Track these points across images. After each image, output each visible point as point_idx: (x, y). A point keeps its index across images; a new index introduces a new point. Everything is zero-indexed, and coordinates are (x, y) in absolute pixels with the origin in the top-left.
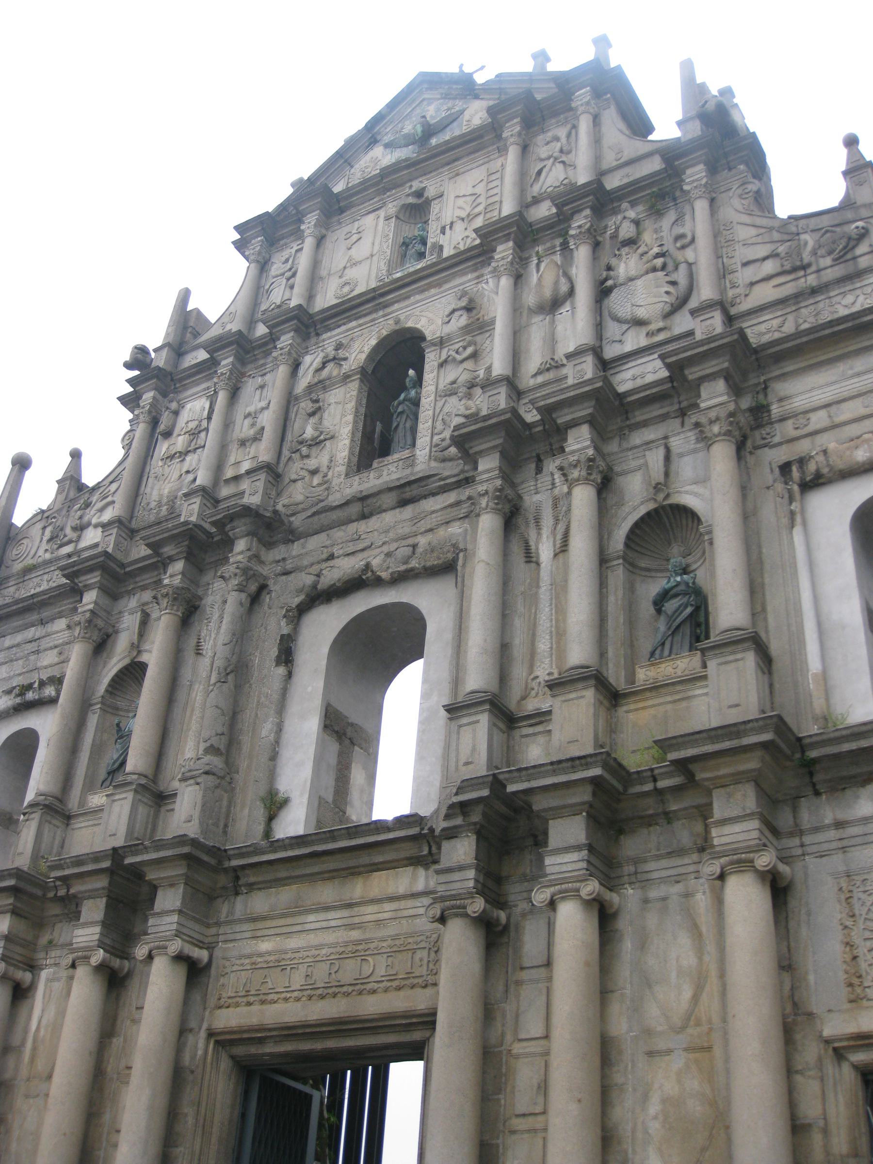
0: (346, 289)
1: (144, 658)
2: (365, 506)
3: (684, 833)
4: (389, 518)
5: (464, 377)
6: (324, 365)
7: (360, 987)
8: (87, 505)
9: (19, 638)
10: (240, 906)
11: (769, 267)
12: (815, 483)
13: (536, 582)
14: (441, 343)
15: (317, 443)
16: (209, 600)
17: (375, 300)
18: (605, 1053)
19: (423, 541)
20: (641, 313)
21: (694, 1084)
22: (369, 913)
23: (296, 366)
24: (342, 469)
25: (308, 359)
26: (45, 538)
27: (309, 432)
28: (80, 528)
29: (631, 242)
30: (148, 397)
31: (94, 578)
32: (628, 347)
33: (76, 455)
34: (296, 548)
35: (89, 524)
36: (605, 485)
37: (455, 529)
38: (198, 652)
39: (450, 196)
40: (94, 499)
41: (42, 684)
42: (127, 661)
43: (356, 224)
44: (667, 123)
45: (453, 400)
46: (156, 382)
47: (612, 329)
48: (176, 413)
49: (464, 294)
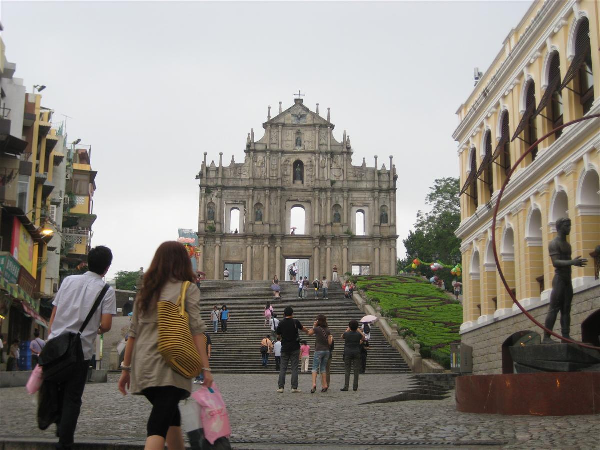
1: (261, 203)
2: (297, 190)
3: (339, 242)
4: (301, 193)
5: (311, 175)
6: (286, 161)
7: (302, 252)
8: (241, 170)
9: (232, 192)
10: (285, 241)
11: (352, 175)
12: (354, 206)
13: (322, 209)
14: (307, 166)
15: (287, 176)
16: (271, 196)
18: (331, 261)
19: (306, 198)
20: (336, 175)
22: (303, 245)
23: (281, 159)
24: (292, 183)
25: (283, 158)
26: (233, 173)
27: (286, 174)
28: (241, 174)
29: (335, 162)
30: (252, 153)
31: (253, 189)
34: (286, 193)
35: (242, 174)
37: (310, 198)
38: (271, 204)
39: (306, 135)
41: (240, 202)
42: (258, 202)
43: (288, 131)
44: (339, 139)
45: (309, 177)
48: (257, 158)
49: (310, 159)
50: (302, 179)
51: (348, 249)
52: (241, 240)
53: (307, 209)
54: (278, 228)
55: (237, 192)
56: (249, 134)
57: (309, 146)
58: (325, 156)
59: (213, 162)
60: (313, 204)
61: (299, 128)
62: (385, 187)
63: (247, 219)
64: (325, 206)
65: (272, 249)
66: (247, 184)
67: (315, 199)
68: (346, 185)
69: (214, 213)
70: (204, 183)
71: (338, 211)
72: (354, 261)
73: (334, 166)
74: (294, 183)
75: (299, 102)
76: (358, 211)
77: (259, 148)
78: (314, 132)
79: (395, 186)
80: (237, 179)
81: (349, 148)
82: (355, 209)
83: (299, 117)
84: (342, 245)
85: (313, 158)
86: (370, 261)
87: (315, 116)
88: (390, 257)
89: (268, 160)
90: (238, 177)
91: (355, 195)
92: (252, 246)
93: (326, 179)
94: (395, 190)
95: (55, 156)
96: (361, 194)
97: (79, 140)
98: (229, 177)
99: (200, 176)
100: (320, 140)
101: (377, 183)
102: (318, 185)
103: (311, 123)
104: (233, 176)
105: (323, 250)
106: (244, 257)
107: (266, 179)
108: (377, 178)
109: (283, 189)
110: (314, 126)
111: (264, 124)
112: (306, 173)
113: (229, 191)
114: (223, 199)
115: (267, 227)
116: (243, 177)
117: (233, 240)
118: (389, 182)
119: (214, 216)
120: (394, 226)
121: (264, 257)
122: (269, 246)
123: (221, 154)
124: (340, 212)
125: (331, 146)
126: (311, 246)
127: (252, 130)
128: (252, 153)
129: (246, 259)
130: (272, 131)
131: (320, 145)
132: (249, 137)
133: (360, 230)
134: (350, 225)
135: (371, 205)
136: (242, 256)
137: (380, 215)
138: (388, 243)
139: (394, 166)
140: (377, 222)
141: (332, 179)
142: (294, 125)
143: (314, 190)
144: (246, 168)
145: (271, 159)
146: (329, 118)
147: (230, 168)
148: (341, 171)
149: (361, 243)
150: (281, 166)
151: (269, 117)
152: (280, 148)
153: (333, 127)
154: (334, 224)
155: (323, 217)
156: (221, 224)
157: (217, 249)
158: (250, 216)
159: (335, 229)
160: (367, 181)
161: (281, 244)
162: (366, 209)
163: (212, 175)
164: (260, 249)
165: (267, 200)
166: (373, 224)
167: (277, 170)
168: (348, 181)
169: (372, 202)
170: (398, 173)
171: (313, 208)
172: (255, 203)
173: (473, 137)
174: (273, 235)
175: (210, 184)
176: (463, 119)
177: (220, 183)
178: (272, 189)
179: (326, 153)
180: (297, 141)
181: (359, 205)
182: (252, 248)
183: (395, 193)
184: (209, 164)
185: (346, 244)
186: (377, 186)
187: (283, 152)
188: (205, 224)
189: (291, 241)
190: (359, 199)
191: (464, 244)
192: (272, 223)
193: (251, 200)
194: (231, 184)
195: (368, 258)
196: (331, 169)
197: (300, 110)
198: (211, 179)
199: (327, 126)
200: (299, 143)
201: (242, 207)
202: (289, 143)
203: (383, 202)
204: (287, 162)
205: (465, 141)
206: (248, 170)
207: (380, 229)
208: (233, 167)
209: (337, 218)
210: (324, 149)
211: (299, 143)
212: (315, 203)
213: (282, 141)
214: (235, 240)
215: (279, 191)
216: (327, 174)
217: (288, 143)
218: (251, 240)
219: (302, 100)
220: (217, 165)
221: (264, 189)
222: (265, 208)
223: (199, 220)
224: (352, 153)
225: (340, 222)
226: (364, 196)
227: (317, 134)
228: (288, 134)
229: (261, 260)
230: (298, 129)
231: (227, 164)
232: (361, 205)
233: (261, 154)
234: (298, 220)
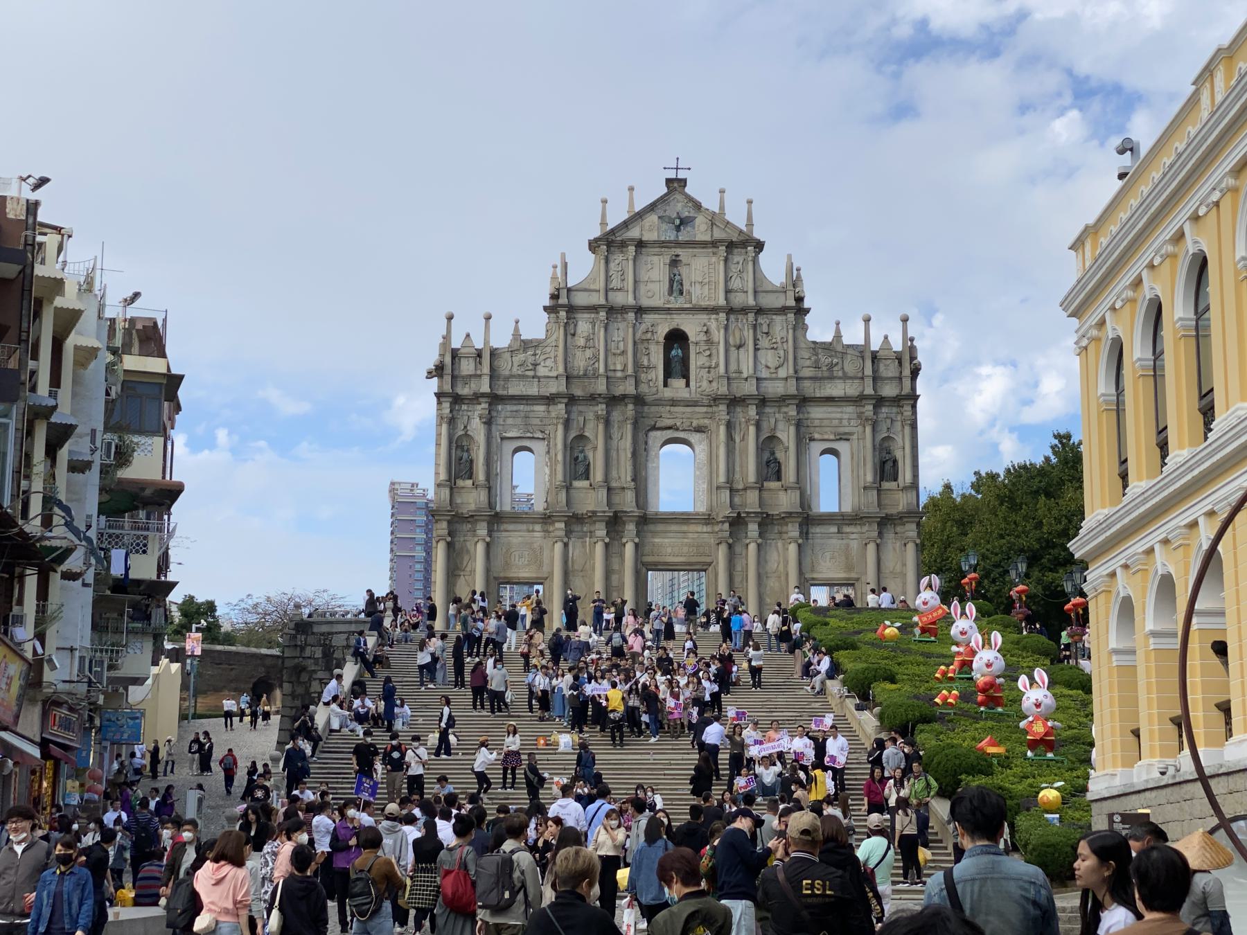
0: (650, 294)
1: (586, 434)
2: (674, 402)
5: (707, 364)
8: (535, 355)
9: (515, 408)
11: (808, 363)
15: (648, 368)
17: (668, 311)
18: (760, 577)
21: (777, 584)
22: (690, 535)
27: (646, 363)
28: (535, 365)
31: (565, 400)
32: (764, 375)
33: (517, 322)
36: (758, 426)
37: (707, 421)
38: (611, 438)
40: (538, 352)
46: (562, 305)
47: (760, 367)
50: (686, 376)
51: (799, 546)
52: (538, 527)
53: (697, 451)
54: (630, 496)
55: (528, 408)
56: (555, 267)
57: (699, 294)
58: (740, 317)
59: (468, 335)
60: (714, 436)
61: (678, 251)
62: (889, 390)
63: (553, 473)
64: (743, 439)
65: (615, 548)
66: (553, 388)
67: (718, 426)
68: (792, 389)
69: (472, 461)
70: (447, 388)
71: (773, 453)
72: (815, 576)
73: (764, 342)
74: (666, 385)
75: (676, 185)
76: (824, 452)
77: (580, 299)
78: (714, 259)
79: (914, 388)
80: (527, 377)
81: (799, 300)
82: (816, 447)
83: (677, 222)
84: (785, 536)
85: (713, 325)
86: (854, 575)
87: (715, 220)
88: (904, 565)
89: (602, 330)
90: (531, 373)
91: (817, 413)
92: (566, 540)
93: (745, 375)
94: (913, 397)
95: (76, 347)
96: (830, 409)
97: (136, 295)
98: (507, 373)
99: (438, 371)
100: (727, 279)
101: (869, 382)
102: (723, 390)
103: (707, 238)
104: (515, 371)
105: (738, 549)
106: (545, 569)
107: (596, 376)
108: (868, 371)
109: (639, 400)
110: (714, 244)
111: (590, 243)
112: (695, 361)
113: (509, 408)
114: (494, 427)
115: (603, 493)
116: (542, 371)
117: (519, 527)
118: (900, 379)
119: (471, 468)
120: (915, 486)
121: (593, 569)
122: (607, 540)
123: (488, 318)
124: (780, 455)
125: (755, 292)
126: (712, 541)
127: (563, 255)
128: (563, 314)
129: (552, 573)
130: (612, 257)
131: (728, 292)
132: (555, 273)
133: (827, 501)
134: (802, 487)
135: (855, 437)
136: (541, 565)
137: (877, 460)
138: (899, 529)
139: (912, 340)
140: (869, 478)
141: (759, 375)
142: (663, 242)
143: (716, 400)
144: (548, 349)
145: (611, 327)
146: (750, 224)
147: (512, 351)
148: (782, 353)
149: (834, 529)
150: (635, 343)
151: (603, 223)
152: (631, 301)
153: (759, 246)
154: (765, 484)
155: (737, 469)
156: (489, 488)
157: (480, 548)
158: (560, 468)
159: (765, 494)
160: (845, 377)
161: (638, 535)
162: (842, 447)
163: (467, 367)
164: (584, 547)
165: (601, 427)
166: (862, 484)
167: (624, 353)
168: (798, 379)
169: (860, 429)
170: (921, 358)
171: (714, 445)
172: (572, 434)
173: (1113, 309)
174: (615, 512)
175: (464, 391)
176: (1087, 264)
177: (485, 388)
178: (614, 401)
179: (744, 310)
180: (671, 281)
181: (826, 437)
182: (566, 545)
183: (914, 407)
184: (456, 343)
185: (797, 534)
186: (869, 391)
187: (640, 311)
188: (451, 489)
189: (660, 527)
190: (826, 423)
191: (1095, 575)
192: (614, 484)
193: (560, 428)
194: (513, 391)
195: (849, 568)
196: (756, 350)
197: (679, 207)
198: (463, 377)
199: (744, 245)
200: (675, 286)
201: (539, 447)
202: (654, 287)
203: (885, 429)
204: (649, 336)
205: (1094, 319)
206: (552, 355)
207: (879, 495)
208: (517, 345)
209: (771, 469)
210: (738, 300)
211: (675, 286)
212: (718, 435)
213: (636, 282)
214: (524, 527)
215: (631, 407)
216: (746, 363)
217: (650, 286)
218: (562, 525)
219: (685, 181)
220: (479, 344)
221: (592, 398)
222: (595, 448)
223: (436, 479)
224: (808, 311)
225: (779, 479)
226: (838, 416)
227: (722, 263)
228: (649, 266)
229: (587, 572)
230: (675, 249)
231: (501, 340)
232: (832, 437)
233: (586, 315)
234: (679, 478)
